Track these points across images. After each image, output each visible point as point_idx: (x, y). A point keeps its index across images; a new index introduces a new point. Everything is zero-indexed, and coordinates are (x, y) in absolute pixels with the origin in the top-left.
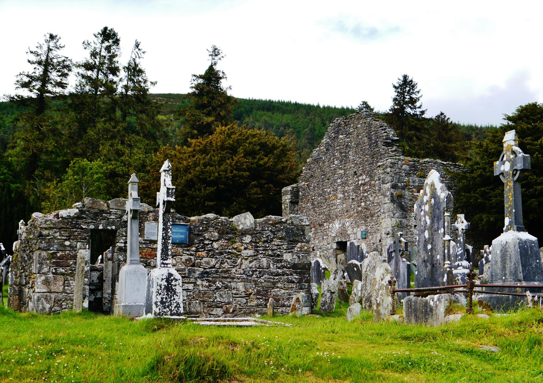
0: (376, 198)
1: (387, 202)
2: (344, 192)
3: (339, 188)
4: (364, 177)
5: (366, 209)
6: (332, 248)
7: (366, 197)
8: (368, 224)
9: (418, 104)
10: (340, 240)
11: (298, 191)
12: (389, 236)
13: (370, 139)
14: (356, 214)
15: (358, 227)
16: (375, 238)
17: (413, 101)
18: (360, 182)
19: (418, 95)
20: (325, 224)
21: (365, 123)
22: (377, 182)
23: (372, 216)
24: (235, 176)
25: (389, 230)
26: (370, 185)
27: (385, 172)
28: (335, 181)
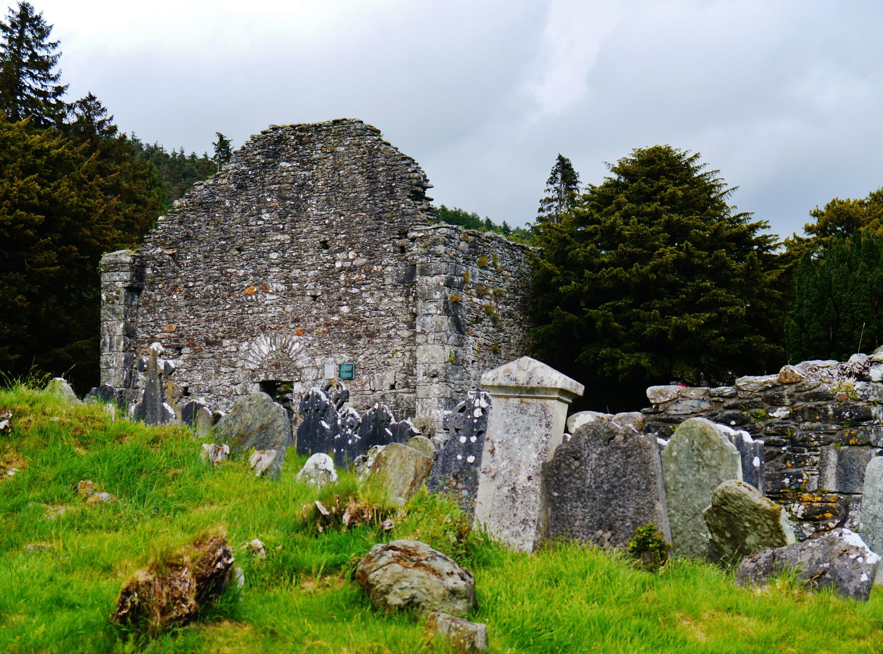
0: (386, 300)
1: (433, 311)
2: (288, 281)
3: (275, 269)
4: (351, 255)
5: (355, 320)
7: (353, 296)
8: (360, 351)
9: (53, 72)
11: (143, 266)
12: (436, 380)
13: (372, 179)
14: (321, 329)
15: (328, 354)
16: (377, 381)
17: (44, 65)
18: (338, 265)
19: (53, 52)
20: (226, 342)
21: (359, 145)
22: (389, 269)
23: (372, 335)
24: (16, 221)
25: (438, 367)
26: (368, 273)
27: (429, 252)
28: (263, 255)
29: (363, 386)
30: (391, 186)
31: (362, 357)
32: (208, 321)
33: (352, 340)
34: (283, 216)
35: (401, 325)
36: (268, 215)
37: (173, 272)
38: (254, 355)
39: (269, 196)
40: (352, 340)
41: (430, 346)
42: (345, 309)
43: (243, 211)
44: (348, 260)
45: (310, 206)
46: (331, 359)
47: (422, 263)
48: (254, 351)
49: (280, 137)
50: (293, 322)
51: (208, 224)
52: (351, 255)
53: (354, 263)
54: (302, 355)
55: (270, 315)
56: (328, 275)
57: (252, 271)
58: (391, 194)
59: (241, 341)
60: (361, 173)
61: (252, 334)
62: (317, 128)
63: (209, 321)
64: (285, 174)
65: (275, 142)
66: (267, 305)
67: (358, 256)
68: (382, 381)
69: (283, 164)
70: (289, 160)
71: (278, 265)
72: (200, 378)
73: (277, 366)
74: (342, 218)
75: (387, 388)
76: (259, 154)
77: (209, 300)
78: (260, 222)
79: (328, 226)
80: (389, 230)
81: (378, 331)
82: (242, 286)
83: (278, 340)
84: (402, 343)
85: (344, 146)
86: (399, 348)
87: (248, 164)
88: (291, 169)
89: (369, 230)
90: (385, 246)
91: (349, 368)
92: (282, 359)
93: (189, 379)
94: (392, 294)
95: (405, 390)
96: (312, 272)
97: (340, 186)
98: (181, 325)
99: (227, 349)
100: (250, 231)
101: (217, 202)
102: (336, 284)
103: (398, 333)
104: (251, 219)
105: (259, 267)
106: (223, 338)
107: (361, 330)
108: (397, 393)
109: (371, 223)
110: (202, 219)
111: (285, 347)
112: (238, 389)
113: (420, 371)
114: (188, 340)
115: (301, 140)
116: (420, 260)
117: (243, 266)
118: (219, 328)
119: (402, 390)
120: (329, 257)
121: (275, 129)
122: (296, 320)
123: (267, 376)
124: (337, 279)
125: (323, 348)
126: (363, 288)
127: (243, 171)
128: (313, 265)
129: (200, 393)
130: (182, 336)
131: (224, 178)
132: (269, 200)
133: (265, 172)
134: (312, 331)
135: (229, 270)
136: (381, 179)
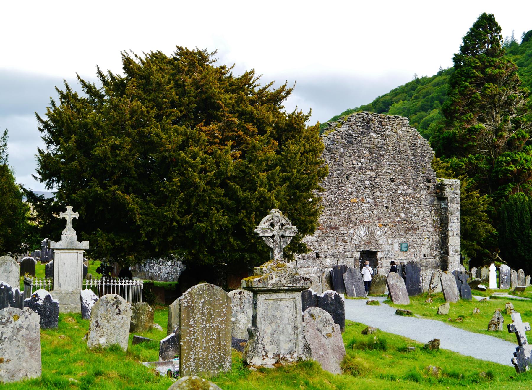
0: (422, 212)
1: (456, 221)
4: (406, 187)
5: (407, 221)
6: (352, 256)
7: (407, 209)
8: (410, 237)
10: (367, 249)
12: (457, 254)
14: (391, 225)
15: (394, 237)
16: (418, 253)
18: (399, 192)
20: (341, 228)
21: (408, 132)
22: (423, 197)
23: (415, 229)
26: (413, 198)
27: (454, 192)
31: (411, 240)
33: (406, 231)
35: (429, 225)
40: (406, 231)
42: (403, 215)
43: (350, 156)
44: (403, 190)
46: (396, 240)
50: (377, 220)
52: (406, 187)
53: (407, 192)
55: (365, 215)
56: (394, 197)
57: (355, 190)
58: (423, 160)
60: (409, 146)
63: (331, 215)
64: (372, 139)
66: (363, 209)
68: (420, 252)
69: (372, 134)
70: (375, 132)
71: (369, 188)
73: (369, 243)
78: (359, 164)
79: (394, 171)
81: (419, 227)
83: (370, 229)
84: (429, 234)
86: (428, 236)
87: (354, 130)
91: (406, 245)
92: (371, 238)
93: (320, 248)
95: (431, 257)
97: (398, 152)
99: (342, 232)
100: (354, 168)
102: (398, 202)
104: (354, 161)
105: (359, 188)
107: (410, 226)
110: (327, 157)
112: (348, 254)
113: (451, 249)
117: (350, 187)
118: (336, 220)
120: (395, 187)
122: (379, 219)
123: (365, 248)
124: (398, 199)
126: (411, 205)
128: (387, 190)
132: (364, 152)
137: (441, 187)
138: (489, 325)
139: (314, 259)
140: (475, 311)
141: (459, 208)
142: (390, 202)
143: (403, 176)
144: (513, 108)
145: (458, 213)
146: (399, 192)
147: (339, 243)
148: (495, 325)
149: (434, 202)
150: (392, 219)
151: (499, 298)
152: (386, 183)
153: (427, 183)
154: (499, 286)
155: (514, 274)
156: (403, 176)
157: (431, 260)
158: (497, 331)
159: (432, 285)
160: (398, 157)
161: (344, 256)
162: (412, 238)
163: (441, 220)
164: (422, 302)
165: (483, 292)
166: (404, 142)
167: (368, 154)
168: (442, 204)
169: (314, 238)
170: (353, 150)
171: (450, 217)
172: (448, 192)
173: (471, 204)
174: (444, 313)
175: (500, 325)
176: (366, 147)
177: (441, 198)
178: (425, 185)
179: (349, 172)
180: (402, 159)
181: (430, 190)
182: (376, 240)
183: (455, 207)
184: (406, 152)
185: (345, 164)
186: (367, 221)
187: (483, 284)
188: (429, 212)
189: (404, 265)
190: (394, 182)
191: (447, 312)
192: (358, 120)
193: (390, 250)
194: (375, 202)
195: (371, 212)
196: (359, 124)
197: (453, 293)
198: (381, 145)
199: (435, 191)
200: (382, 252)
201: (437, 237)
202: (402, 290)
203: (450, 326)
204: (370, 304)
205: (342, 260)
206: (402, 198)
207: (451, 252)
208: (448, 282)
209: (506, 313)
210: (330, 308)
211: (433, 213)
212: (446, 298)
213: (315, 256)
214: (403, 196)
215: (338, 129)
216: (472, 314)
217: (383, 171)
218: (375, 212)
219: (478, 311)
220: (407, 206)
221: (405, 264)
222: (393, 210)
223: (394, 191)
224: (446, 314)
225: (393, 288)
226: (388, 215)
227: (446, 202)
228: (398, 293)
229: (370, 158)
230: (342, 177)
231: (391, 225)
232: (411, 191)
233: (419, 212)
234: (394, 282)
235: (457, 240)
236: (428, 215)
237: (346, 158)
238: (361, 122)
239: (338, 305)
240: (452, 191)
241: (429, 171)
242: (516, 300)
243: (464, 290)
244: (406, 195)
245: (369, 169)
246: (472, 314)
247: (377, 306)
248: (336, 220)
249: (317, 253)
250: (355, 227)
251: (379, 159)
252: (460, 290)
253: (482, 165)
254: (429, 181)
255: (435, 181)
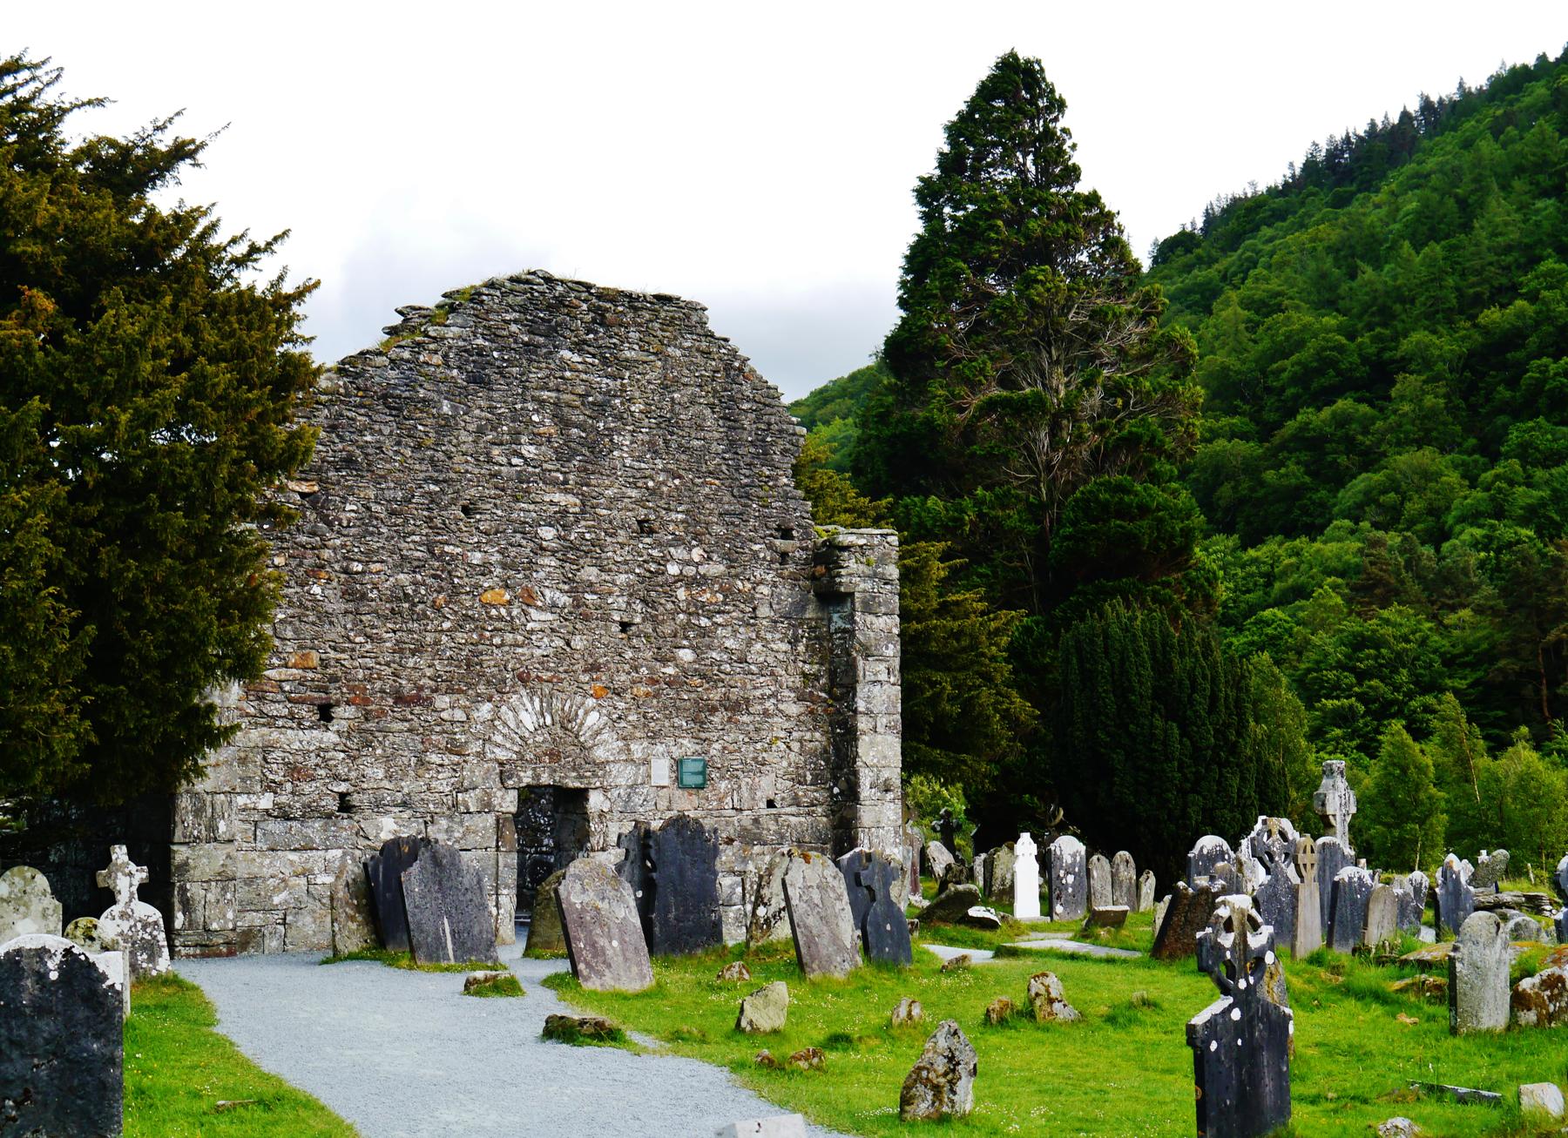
0: (758, 646)
1: (883, 677)
2: (576, 588)
4: (697, 554)
5: (703, 677)
6: (487, 807)
7: (703, 632)
8: (714, 735)
10: (545, 779)
12: (890, 796)
13: (730, 422)
14: (642, 689)
15: (654, 737)
16: (745, 794)
18: (673, 569)
20: (442, 701)
22: (765, 590)
23: (735, 707)
26: (727, 592)
27: (875, 575)
29: (720, 800)
30: (764, 441)
32: (399, 649)
33: (700, 714)
34: (562, 457)
35: (786, 693)
36: (532, 448)
37: (313, 534)
38: (505, 731)
39: (537, 411)
40: (700, 714)
41: (879, 738)
42: (686, 655)
43: (480, 431)
44: (688, 563)
45: (620, 447)
46: (660, 748)
47: (864, 591)
48: (505, 724)
49: (561, 300)
50: (585, 671)
51: (398, 443)
52: (697, 554)
53: (702, 570)
54: (605, 736)
55: (538, 652)
56: (651, 589)
57: (498, 557)
58: (765, 457)
59: (479, 699)
60: (712, 406)
61: (499, 688)
62: (631, 299)
63: (401, 651)
64: (568, 374)
65: (550, 306)
66: (532, 632)
67: (710, 558)
68: (753, 790)
69: (566, 354)
70: (578, 347)
71: (554, 553)
72: (381, 774)
73: (554, 756)
74: (677, 482)
75: (763, 805)
76: (515, 321)
77: (402, 605)
78: (515, 461)
79: (652, 492)
80: (764, 519)
81: (747, 701)
82: (477, 586)
83: (557, 704)
85: (681, 347)
86: (782, 734)
87: (493, 336)
88: (580, 367)
89: (727, 513)
90: (756, 547)
91: (699, 767)
92: (564, 740)
93: (353, 775)
94: (769, 636)
95: (794, 809)
96: (623, 577)
97: (669, 424)
98: (332, 654)
99: (444, 715)
100: (495, 476)
101: (424, 400)
102: (670, 606)
103: (781, 707)
104: (496, 451)
105: (513, 551)
106: (435, 691)
107: (716, 695)
108: (779, 815)
109: (729, 503)
110: (386, 431)
111: (566, 722)
112: (471, 800)
113: (865, 779)
114: (352, 690)
115: (603, 316)
116: (862, 586)
117: (478, 547)
118: (422, 668)
119: (788, 810)
120: (655, 553)
121: (549, 280)
122: (594, 668)
123: (537, 776)
124: (670, 596)
125: (645, 726)
126: (719, 619)
127: (480, 351)
128: (626, 562)
129: (379, 806)
130: (334, 679)
131: (436, 352)
133: (530, 361)
134: (625, 691)
135: (447, 549)
136: (746, 424)
137: (829, 555)
138: (907, 1088)
139: (329, 816)
140: (903, 1012)
141: (896, 631)
142: (639, 607)
143: (687, 512)
144: (1105, 347)
145: (892, 651)
146: (673, 569)
147: (434, 758)
148: (937, 1089)
149: (804, 609)
150: (644, 670)
151: (1027, 953)
152: (622, 536)
153: (778, 542)
154: (1048, 911)
155: (1100, 866)
156: (687, 512)
157: (795, 820)
158: (942, 1120)
159: (761, 911)
160: (666, 442)
161: (455, 805)
162: (723, 740)
163: (832, 674)
164: (710, 977)
165: (987, 935)
166: (690, 390)
167: (549, 427)
168: (835, 617)
169: (330, 737)
170: (491, 409)
171: (860, 663)
172: (852, 574)
173: (957, 635)
174: (765, 1024)
175: (961, 1086)
176: (541, 402)
177: (831, 596)
178: (770, 547)
179: (473, 491)
180: (685, 450)
181: (791, 568)
182: (583, 747)
183: (880, 628)
184: (700, 428)
185: (456, 460)
186: (546, 675)
187: (985, 904)
188: (785, 647)
189: (648, 833)
190: (651, 532)
191: (779, 1022)
192: (510, 299)
193: (634, 782)
194: (578, 603)
195: (561, 643)
196: (516, 315)
197: (835, 939)
198: (600, 398)
199: (809, 570)
200: (605, 790)
201: (817, 735)
202: (623, 932)
203: (744, 1094)
204: (478, 993)
205: (444, 823)
206: (682, 594)
207: (865, 792)
208: (816, 896)
209: (1031, 1015)
210: (32, 1030)
211: (801, 648)
212: (806, 959)
213: (332, 804)
214: (688, 586)
215: (432, 331)
216: (889, 1025)
217: (609, 492)
218: (578, 642)
219: (916, 1011)
220: (704, 622)
221: (656, 825)
222: (647, 636)
223: (653, 567)
224: (775, 1032)
225: (582, 923)
226: (629, 654)
227: (848, 609)
228: (602, 942)
229: (558, 441)
230: (446, 508)
231: (642, 689)
232: (716, 568)
233: (749, 643)
234: (590, 897)
235: (891, 746)
236: (781, 656)
237: (464, 436)
238: (523, 309)
239: (82, 1013)
240: (867, 571)
241: (786, 497)
242: (1086, 958)
243: (879, 927)
244: (699, 581)
245: (555, 482)
246: (889, 1025)
247: (501, 1002)
248: (422, 668)
249: (342, 796)
250: (497, 697)
251: (595, 450)
252: (861, 922)
253: (1013, 518)
254: (786, 534)
255: (807, 535)
